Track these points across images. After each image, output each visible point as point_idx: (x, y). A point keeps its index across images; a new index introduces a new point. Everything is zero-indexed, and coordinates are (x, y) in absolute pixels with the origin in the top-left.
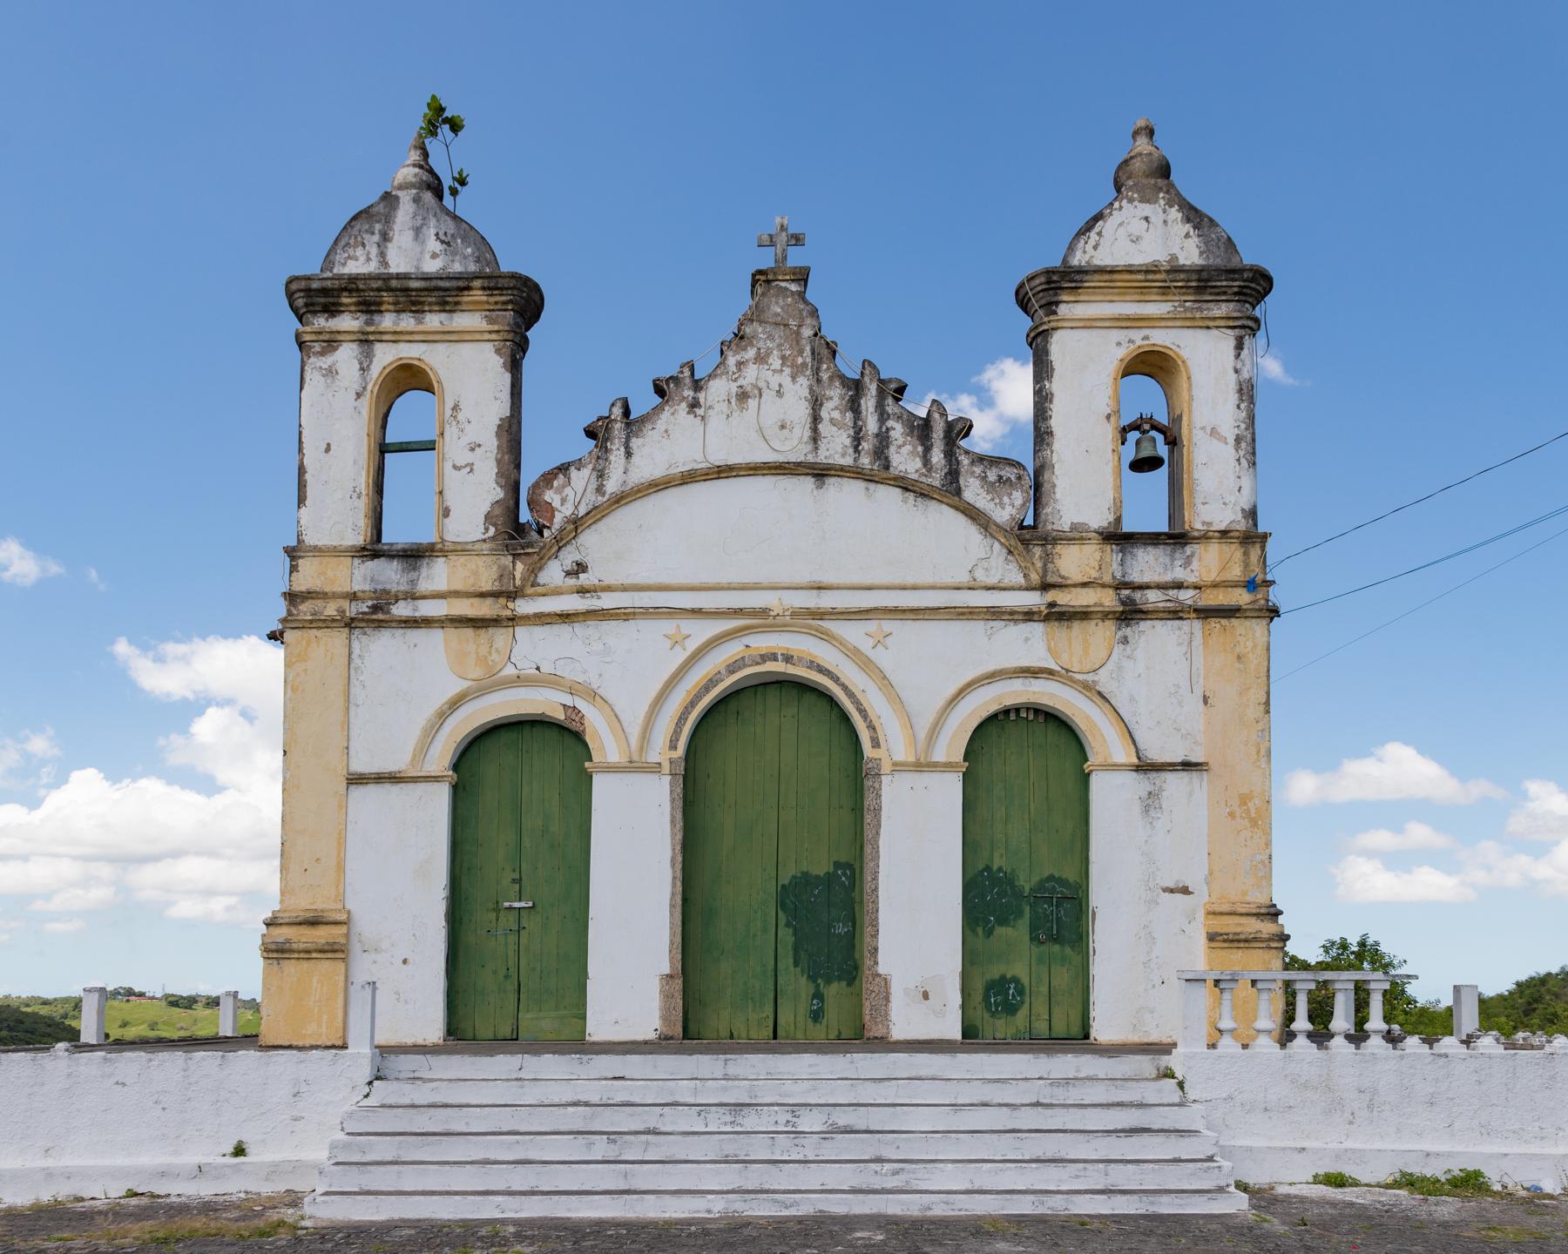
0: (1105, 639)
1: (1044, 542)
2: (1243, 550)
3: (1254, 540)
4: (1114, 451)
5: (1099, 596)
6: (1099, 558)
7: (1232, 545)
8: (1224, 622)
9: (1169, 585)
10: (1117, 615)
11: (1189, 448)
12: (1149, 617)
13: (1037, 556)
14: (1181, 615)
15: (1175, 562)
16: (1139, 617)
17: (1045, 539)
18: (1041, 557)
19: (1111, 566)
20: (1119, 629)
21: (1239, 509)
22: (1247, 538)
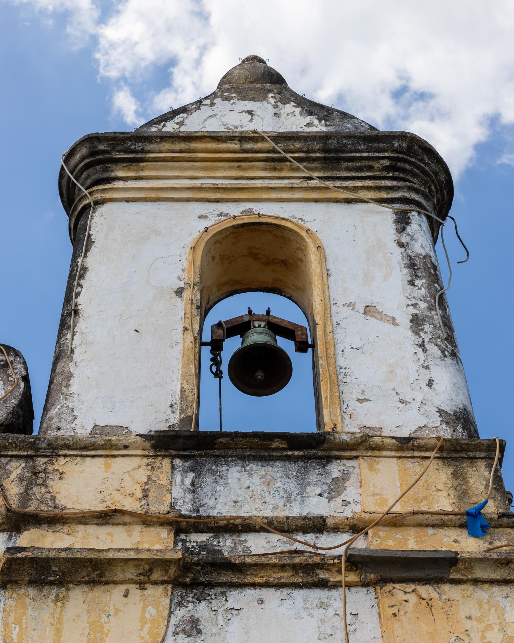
0: (143, 621)
1: (30, 453)
2: (450, 470)
3: (472, 454)
4: (185, 329)
5: (139, 539)
6: (146, 480)
7: (426, 463)
8: (425, 590)
9: (293, 524)
10: (173, 571)
11: (325, 327)
12: (250, 579)
13: (13, 476)
14: (323, 575)
15: (309, 489)
16: (224, 579)
17: (34, 446)
18: (21, 478)
19: (170, 491)
20: (180, 604)
21: (433, 410)
22: (456, 451)
